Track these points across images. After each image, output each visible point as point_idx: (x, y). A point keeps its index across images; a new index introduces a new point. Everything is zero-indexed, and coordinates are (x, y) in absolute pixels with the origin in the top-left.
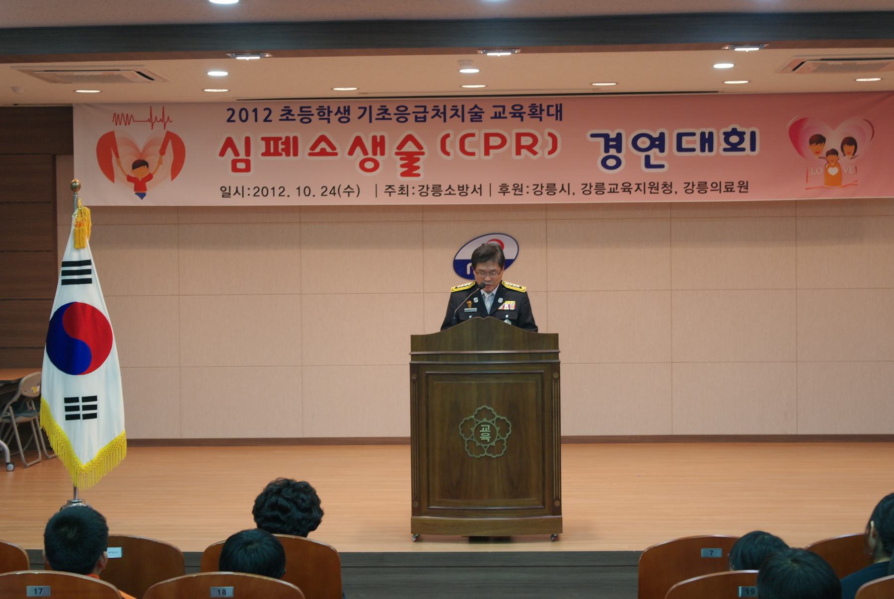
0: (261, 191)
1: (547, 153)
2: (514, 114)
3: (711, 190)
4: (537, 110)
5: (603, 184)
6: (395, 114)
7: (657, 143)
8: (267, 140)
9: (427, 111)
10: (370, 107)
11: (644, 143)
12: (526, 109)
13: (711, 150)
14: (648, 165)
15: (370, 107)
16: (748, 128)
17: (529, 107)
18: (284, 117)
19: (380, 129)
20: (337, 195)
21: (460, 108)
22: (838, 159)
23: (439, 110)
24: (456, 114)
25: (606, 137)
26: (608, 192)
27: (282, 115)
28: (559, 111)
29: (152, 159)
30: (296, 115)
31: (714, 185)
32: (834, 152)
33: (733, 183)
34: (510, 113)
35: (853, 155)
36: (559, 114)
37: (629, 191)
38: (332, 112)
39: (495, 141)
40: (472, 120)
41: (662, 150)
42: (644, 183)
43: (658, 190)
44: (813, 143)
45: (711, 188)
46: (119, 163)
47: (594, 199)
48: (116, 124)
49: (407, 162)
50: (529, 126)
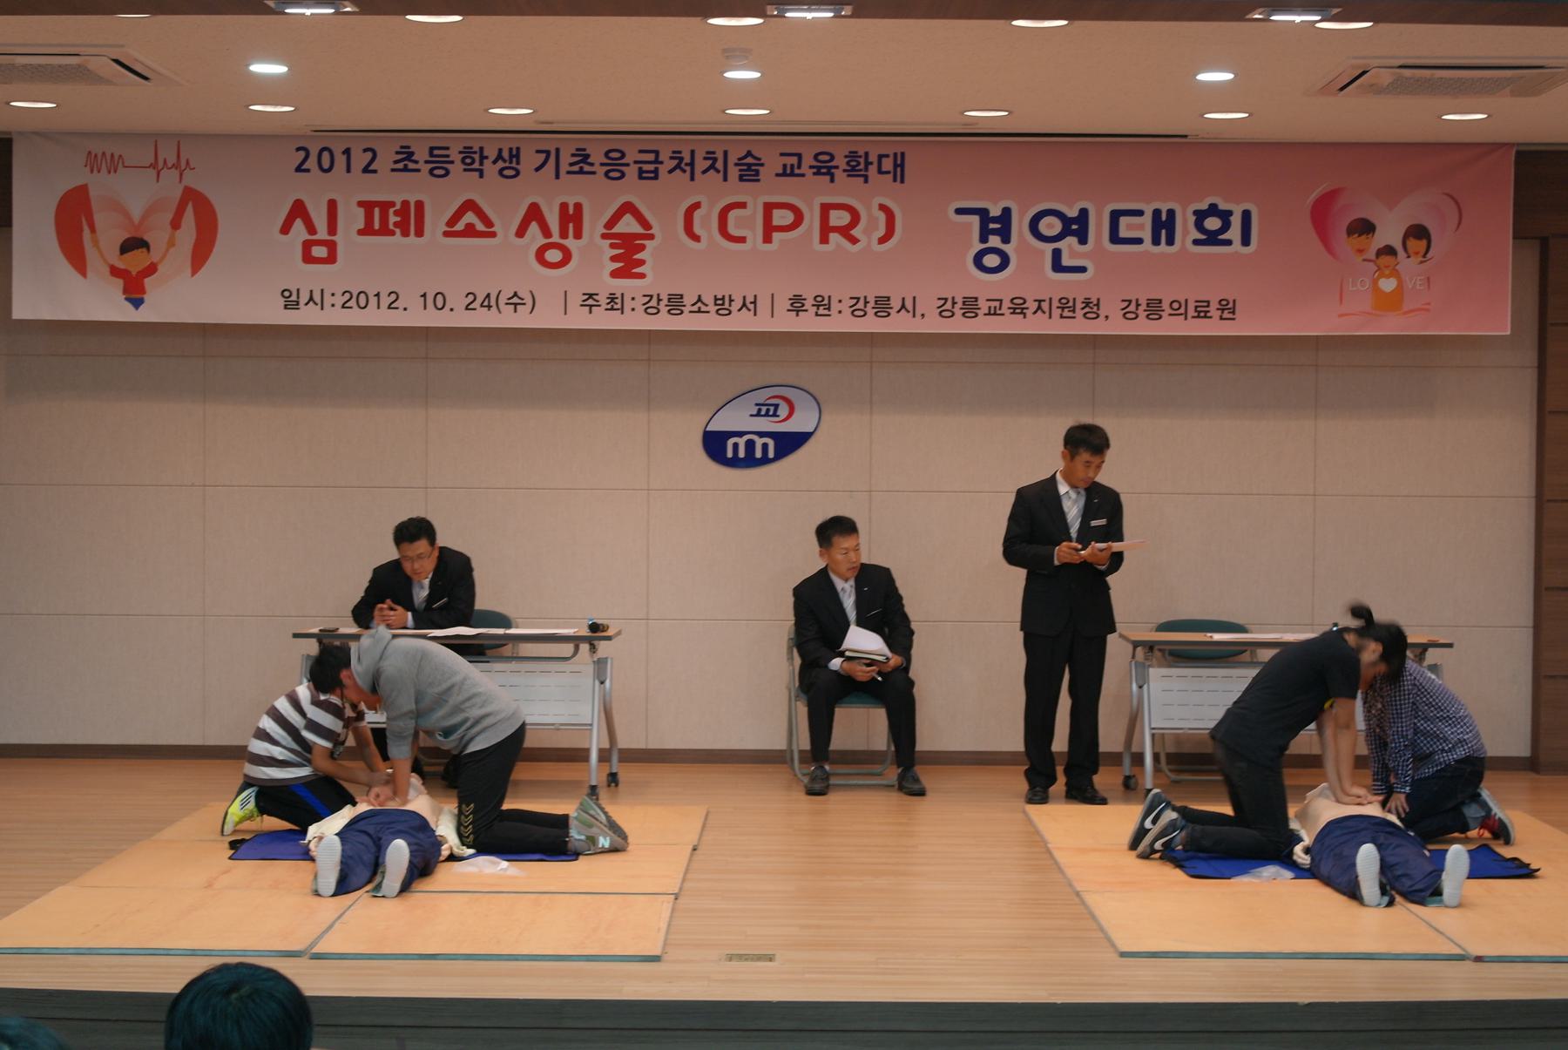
0: (355, 299)
1: (876, 242)
2: (819, 168)
3: (1170, 315)
4: (859, 164)
5: (976, 299)
6: (602, 164)
7: (1074, 227)
8: (368, 206)
9: (660, 159)
10: (558, 150)
11: (1050, 226)
12: (841, 161)
13: (1170, 242)
14: (1058, 266)
15: (558, 150)
17: (846, 157)
18: (400, 166)
19: (573, 191)
20: (494, 309)
21: (720, 156)
22: (1398, 263)
23: (681, 159)
24: (712, 167)
25: (983, 213)
26: (985, 314)
27: (396, 162)
28: (899, 166)
29: (157, 237)
30: (421, 162)
31: (1176, 305)
32: (1389, 251)
33: (1208, 302)
34: (811, 167)
35: (1424, 256)
36: (899, 170)
37: (1021, 313)
38: (487, 157)
39: (782, 217)
40: (741, 179)
41: (1083, 240)
42: (1051, 299)
43: (1074, 311)
44: (1355, 233)
46: (96, 243)
47: (959, 325)
48: (92, 171)
49: (622, 251)
50: (845, 190)
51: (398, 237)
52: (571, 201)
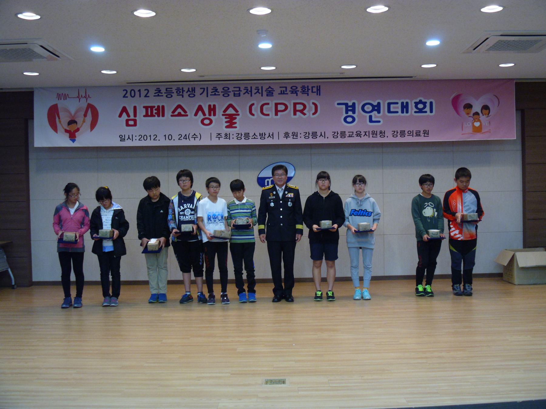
0: (143, 137)
2: (292, 91)
4: (305, 90)
5: (345, 132)
6: (222, 92)
7: (376, 108)
8: (146, 108)
9: (241, 90)
11: (368, 108)
12: (299, 89)
13: (407, 112)
14: (371, 121)
15: (207, 88)
16: (428, 99)
17: (301, 87)
21: (260, 88)
22: (480, 117)
23: (248, 90)
24: (258, 92)
25: (346, 105)
26: (348, 137)
27: (155, 93)
29: (79, 120)
30: (163, 93)
31: (410, 132)
32: (477, 114)
33: (420, 131)
34: (290, 91)
35: (488, 115)
36: (319, 91)
37: (360, 136)
38: (184, 91)
39: (281, 107)
40: (267, 95)
41: (379, 112)
42: (369, 131)
43: (377, 135)
45: (407, 134)
46: (60, 122)
48: (59, 99)
50: (301, 98)
51: (156, 117)
52: (212, 104)
